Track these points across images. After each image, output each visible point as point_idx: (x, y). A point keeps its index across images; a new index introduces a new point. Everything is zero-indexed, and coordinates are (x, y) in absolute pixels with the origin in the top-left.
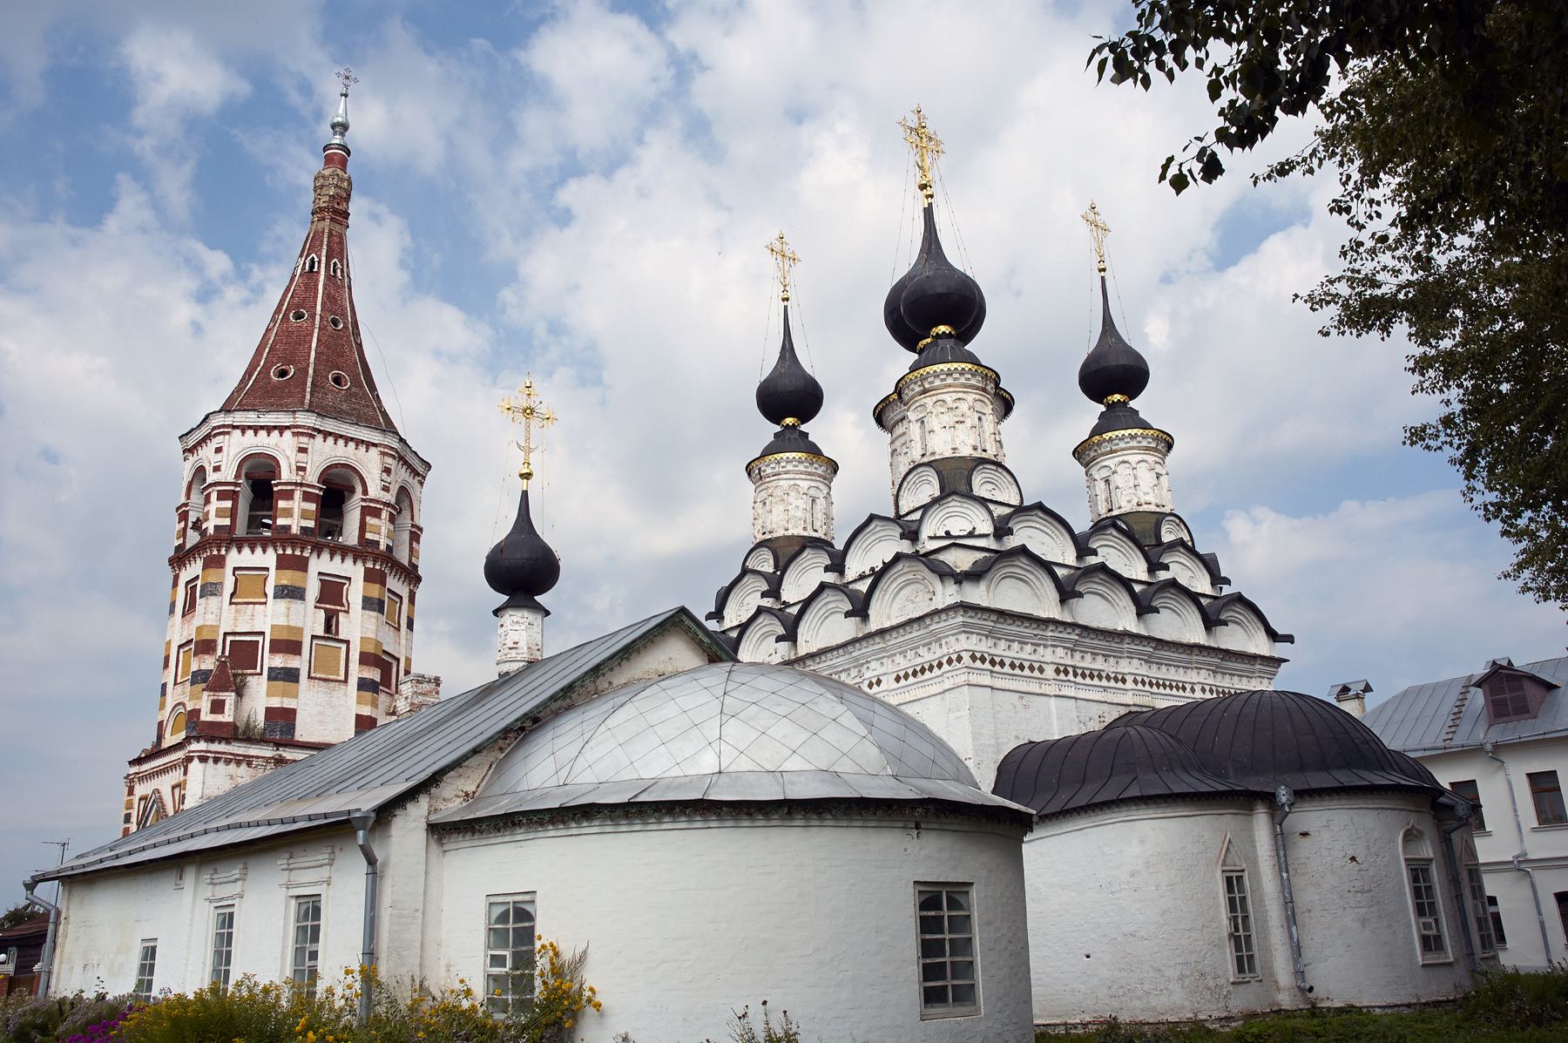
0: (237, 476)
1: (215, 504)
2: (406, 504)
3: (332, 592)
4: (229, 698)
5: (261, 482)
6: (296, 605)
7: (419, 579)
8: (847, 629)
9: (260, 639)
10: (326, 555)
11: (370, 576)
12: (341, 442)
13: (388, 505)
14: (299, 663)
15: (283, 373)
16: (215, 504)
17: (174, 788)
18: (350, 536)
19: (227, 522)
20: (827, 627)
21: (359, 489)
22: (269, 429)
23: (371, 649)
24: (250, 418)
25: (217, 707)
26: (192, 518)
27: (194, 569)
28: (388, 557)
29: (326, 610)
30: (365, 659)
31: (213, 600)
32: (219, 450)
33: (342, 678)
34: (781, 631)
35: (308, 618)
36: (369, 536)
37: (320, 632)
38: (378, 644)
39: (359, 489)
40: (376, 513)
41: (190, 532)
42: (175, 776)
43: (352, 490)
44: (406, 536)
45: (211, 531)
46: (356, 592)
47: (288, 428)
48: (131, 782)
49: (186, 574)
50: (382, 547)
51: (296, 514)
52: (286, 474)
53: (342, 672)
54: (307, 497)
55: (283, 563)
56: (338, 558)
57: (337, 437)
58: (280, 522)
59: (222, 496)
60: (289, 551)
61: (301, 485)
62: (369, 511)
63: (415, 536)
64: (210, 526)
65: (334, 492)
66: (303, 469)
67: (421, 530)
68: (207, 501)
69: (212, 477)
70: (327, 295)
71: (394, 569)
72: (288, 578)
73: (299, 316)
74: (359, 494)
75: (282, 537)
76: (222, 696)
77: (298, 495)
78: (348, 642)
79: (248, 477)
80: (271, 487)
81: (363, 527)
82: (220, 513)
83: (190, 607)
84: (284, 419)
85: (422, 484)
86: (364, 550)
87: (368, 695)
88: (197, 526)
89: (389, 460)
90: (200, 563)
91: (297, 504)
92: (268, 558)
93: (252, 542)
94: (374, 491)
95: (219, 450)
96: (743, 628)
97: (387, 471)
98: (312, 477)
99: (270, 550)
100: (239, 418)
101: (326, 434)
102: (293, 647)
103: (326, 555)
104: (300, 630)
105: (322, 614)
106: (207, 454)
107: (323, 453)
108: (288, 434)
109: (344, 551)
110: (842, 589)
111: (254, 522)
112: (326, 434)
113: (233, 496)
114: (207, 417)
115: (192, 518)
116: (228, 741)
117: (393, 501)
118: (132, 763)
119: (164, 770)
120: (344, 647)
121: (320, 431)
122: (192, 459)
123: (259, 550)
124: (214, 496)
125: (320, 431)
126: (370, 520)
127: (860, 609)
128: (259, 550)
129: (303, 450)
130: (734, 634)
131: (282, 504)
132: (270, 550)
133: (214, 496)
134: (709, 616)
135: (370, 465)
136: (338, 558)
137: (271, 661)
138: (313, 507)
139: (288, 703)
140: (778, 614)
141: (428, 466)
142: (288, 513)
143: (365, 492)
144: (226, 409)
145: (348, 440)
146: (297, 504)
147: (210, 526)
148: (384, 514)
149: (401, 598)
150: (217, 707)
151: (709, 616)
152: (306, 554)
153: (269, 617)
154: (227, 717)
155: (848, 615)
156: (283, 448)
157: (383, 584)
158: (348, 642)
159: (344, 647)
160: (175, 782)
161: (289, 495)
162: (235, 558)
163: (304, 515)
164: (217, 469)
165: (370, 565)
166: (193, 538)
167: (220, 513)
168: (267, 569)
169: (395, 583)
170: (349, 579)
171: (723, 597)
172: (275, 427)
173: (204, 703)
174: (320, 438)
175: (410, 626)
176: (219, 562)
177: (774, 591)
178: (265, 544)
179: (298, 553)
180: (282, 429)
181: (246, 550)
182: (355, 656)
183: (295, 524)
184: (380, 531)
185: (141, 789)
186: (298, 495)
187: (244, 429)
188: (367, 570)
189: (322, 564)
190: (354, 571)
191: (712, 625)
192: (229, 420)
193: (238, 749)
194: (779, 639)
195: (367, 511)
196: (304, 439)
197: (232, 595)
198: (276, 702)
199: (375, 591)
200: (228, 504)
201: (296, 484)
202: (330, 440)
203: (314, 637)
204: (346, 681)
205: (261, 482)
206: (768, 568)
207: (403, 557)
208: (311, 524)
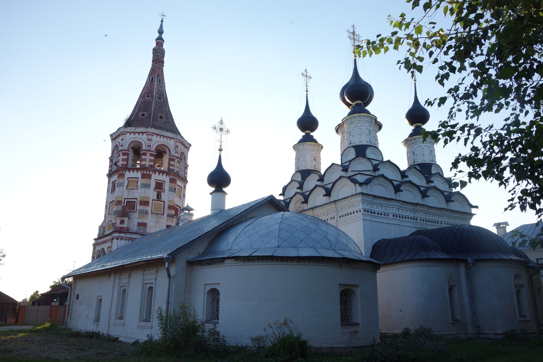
2: (183, 158)
3: (159, 186)
6: (147, 190)
11: (172, 181)
12: (162, 137)
13: (177, 157)
21: (168, 152)
23: (171, 204)
28: (177, 174)
29: (157, 192)
30: (170, 207)
34: (303, 200)
35: (152, 194)
36: (171, 167)
37: (155, 198)
38: (174, 202)
40: (173, 160)
41: (113, 166)
43: (166, 153)
44: (183, 168)
46: (167, 186)
50: (175, 171)
54: (151, 155)
56: (161, 174)
57: (161, 136)
60: (145, 172)
63: (186, 167)
71: (179, 177)
72: (145, 181)
75: (143, 168)
77: (148, 154)
78: (164, 202)
85: (188, 151)
86: (169, 172)
87: (170, 219)
94: (173, 152)
96: (291, 199)
98: (153, 149)
101: (157, 135)
103: (157, 173)
104: (149, 198)
105: (156, 193)
107: (156, 141)
109: (163, 172)
110: (323, 187)
112: (157, 135)
113: (127, 154)
120: (163, 203)
126: (172, 163)
130: (288, 201)
134: (280, 195)
135: (171, 144)
136: (161, 174)
138: (153, 158)
140: (302, 194)
141: (190, 145)
143: (170, 153)
148: (176, 160)
151: (280, 195)
152: (151, 173)
158: (164, 202)
159: (163, 203)
163: (150, 161)
165: (171, 177)
166: (114, 168)
169: (179, 183)
171: (285, 189)
174: (155, 136)
177: (301, 188)
179: (148, 173)
182: (166, 206)
183: (147, 163)
186: (148, 154)
188: (170, 179)
189: (156, 177)
190: (165, 178)
191: (282, 198)
195: (170, 160)
199: (173, 185)
203: (153, 200)
204: (163, 214)
206: (299, 179)
207: (181, 174)
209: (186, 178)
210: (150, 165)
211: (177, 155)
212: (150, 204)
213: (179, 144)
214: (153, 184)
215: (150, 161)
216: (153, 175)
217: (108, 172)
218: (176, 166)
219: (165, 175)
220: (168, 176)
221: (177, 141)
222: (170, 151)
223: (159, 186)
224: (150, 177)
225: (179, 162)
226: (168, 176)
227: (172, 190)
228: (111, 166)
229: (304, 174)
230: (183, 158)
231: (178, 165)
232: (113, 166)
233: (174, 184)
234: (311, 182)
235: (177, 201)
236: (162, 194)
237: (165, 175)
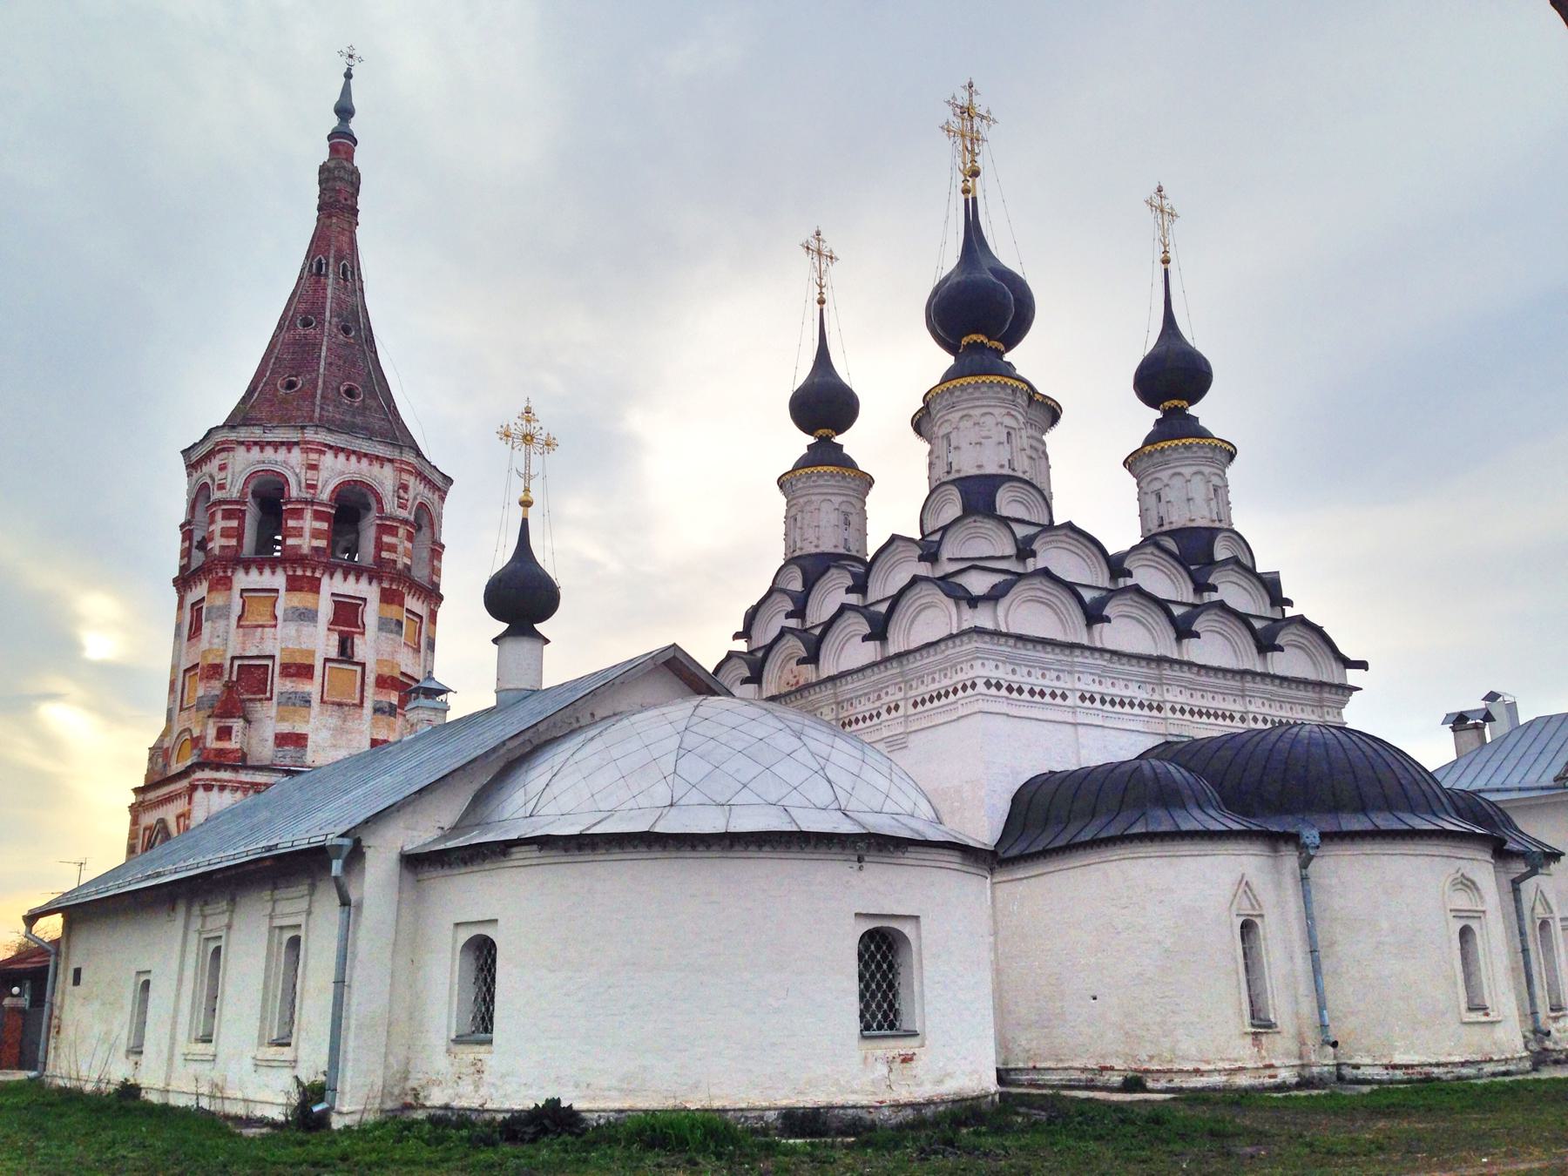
0: (243, 492)
1: (220, 524)
2: (425, 521)
3: (347, 614)
4: (237, 725)
5: (271, 500)
6: (307, 629)
7: (441, 598)
8: (868, 652)
9: (269, 663)
10: (338, 576)
11: (388, 597)
12: (353, 458)
13: (405, 522)
14: (312, 688)
15: (291, 385)
16: (220, 524)
17: (178, 817)
18: (366, 554)
19: (233, 542)
20: (850, 650)
21: (374, 505)
22: (276, 446)
23: (386, 671)
24: (257, 433)
25: (225, 733)
26: (197, 537)
27: (200, 590)
30: (383, 682)
31: (221, 623)
32: (222, 468)
33: (357, 701)
35: (321, 641)
36: (385, 554)
37: (334, 653)
39: (374, 505)
40: (392, 531)
41: (195, 552)
42: (179, 806)
43: (368, 508)
44: (426, 554)
45: (217, 551)
47: (297, 443)
48: (136, 810)
49: (191, 597)
50: (400, 566)
51: (307, 534)
52: (294, 492)
53: (358, 696)
54: (318, 516)
55: (294, 585)
56: (351, 579)
58: (290, 542)
59: (228, 515)
60: (299, 572)
61: (312, 503)
62: (384, 529)
64: (216, 545)
65: (349, 508)
66: (314, 487)
67: (443, 547)
68: (212, 521)
69: (217, 495)
70: (339, 302)
72: (300, 600)
73: (306, 324)
74: (374, 513)
75: (293, 559)
76: (229, 722)
77: (308, 514)
78: (363, 665)
79: (254, 494)
80: (280, 505)
81: (380, 546)
82: (226, 533)
83: (195, 630)
84: (294, 436)
86: (377, 572)
88: (202, 545)
89: (405, 476)
90: (205, 585)
91: (308, 523)
92: (278, 580)
93: (263, 560)
94: (390, 506)
95: (222, 468)
97: (405, 488)
98: (325, 496)
99: (280, 571)
100: (243, 434)
102: (305, 671)
103: (338, 576)
105: (336, 636)
106: (212, 467)
107: (334, 471)
108: (296, 451)
109: (358, 571)
111: (265, 542)
112: (337, 450)
114: (210, 431)
115: (197, 537)
116: (235, 769)
117: (412, 518)
118: (137, 791)
119: (169, 799)
120: (359, 669)
121: (331, 447)
122: (195, 475)
123: (267, 571)
124: (219, 515)
125: (331, 447)
126: (386, 539)
127: (879, 630)
128: (267, 571)
129: (313, 467)
131: (291, 523)
132: (280, 571)
133: (219, 515)
135: (384, 479)
136: (351, 579)
137: (280, 685)
138: (325, 526)
139: (300, 728)
142: (298, 533)
143: (381, 509)
144: (232, 423)
145: (361, 456)
146: (308, 523)
147: (216, 545)
148: (401, 532)
149: (421, 617)
150: (225, 733)
152: (317, 575)
153: (279, 641)
154: (233, 744)
155: (866, 638)
156: (291, 464)
157: (402, 605)
158: (363, 665)
159: (359, 669)
160: (180, 811)
161: (298, 514)
162: (242, 580)
163: (316, 534)
164: (221, 487)
165: (386, 585)
166: (198, 558)
167: (226, 533)
168: (277, 591)
169: (412, 603)
170: (365, 600)
172: (282, 443)
173: (211, 732)
175: (431, 645)
176: (226, 583)
178: (274, 564)
179: (309, 573)
180: (289, 445)
181: (254, 572)
182: (371, 679)
183: (305, 544)
184: (402, 551)
185: (149, 819)
186: (308, 514)
187: (249, 446)
188: (383, 591)
189: (335, 585)
192: (233, 436)
193: (245, 777)
194: (801, 662)
195: (384, 529)
196: (314, 456)
197: (240, 618)
198: (285, 728)
199: (393, 611)
200: (234, 523)
201: (306, 502)
202: (342, 457)
203: (327, 660)
205: (271, 500)
207: (420, 574)
208: (322, 543)
209: (437, 586)
210: (316, 549)
211: (403, 514)
212: (318, 671)
213: (412, 481)
214: (325, 608)
215: (316, 534)
216: (325, 581)
217: (176, 573)
218: (400, 549)
219: (364, 581)
220: (375, 583)
221: (402, 470)
222: (379, 501)
223: (347, 614)
224: (315, 586)
225: (410, 537)
226: (375, 583)
227: (391, 626)
228: (186, 554)
229: (810, 567)
230: (425, 522)
231: (409, 545)
232: (195, 552)
233: (395, 608)
234: (831, 596)
235: (407, 663)
236: (358, 640)
237: (364, 581)
